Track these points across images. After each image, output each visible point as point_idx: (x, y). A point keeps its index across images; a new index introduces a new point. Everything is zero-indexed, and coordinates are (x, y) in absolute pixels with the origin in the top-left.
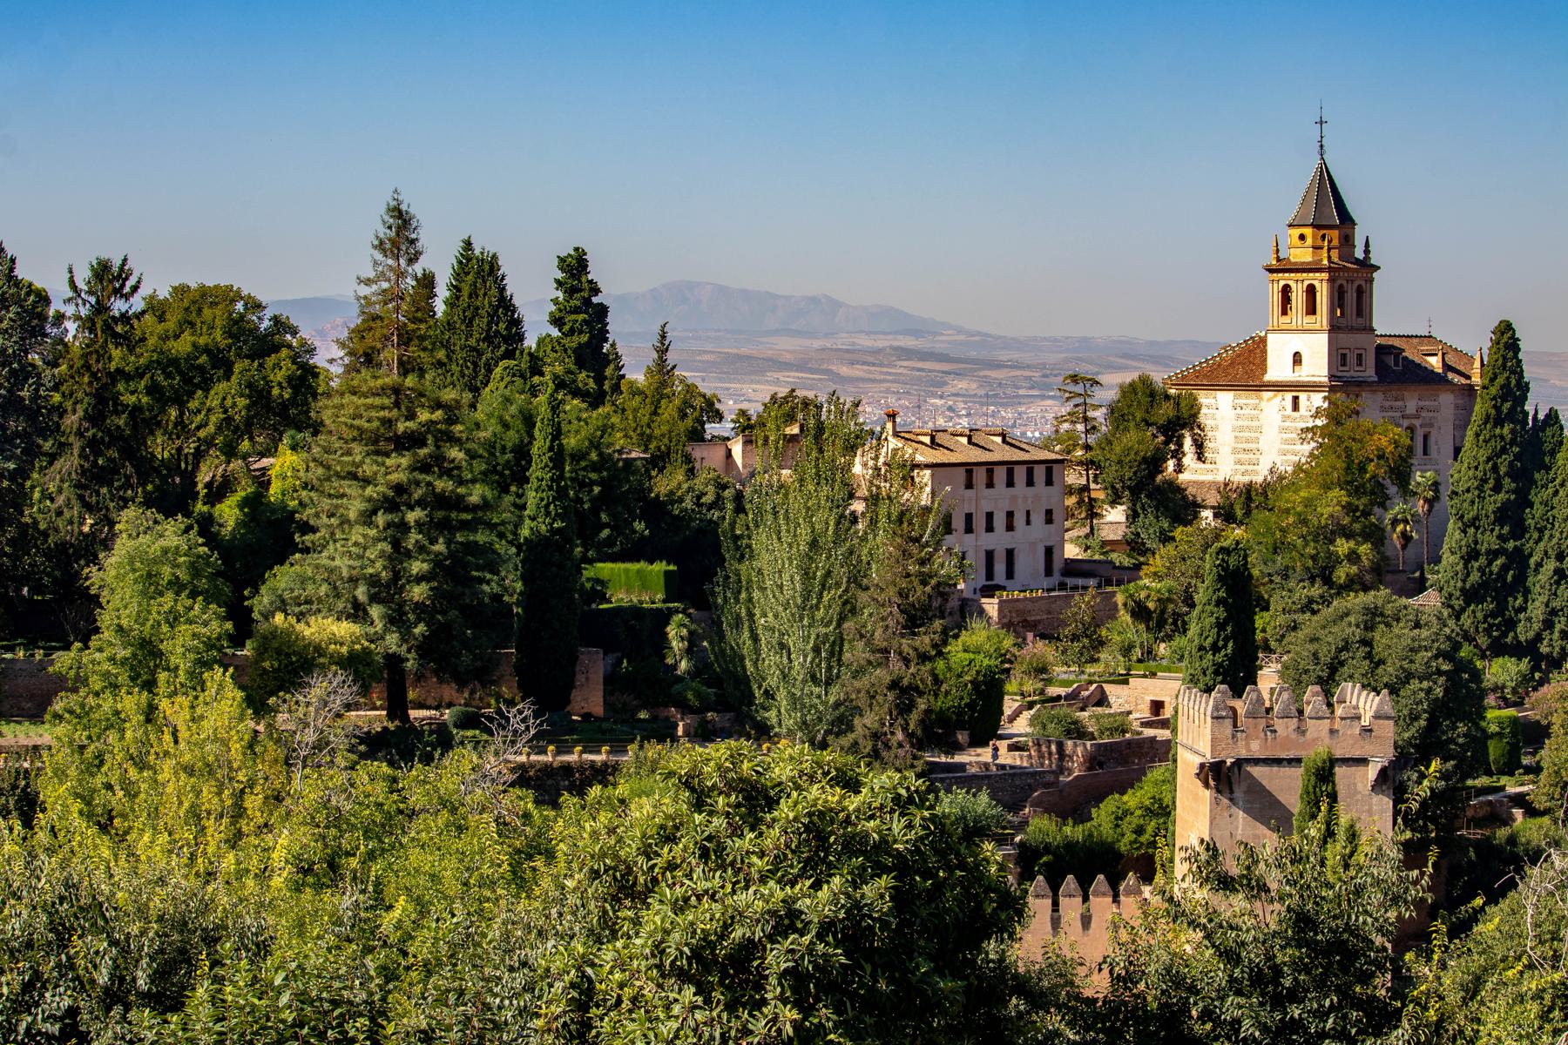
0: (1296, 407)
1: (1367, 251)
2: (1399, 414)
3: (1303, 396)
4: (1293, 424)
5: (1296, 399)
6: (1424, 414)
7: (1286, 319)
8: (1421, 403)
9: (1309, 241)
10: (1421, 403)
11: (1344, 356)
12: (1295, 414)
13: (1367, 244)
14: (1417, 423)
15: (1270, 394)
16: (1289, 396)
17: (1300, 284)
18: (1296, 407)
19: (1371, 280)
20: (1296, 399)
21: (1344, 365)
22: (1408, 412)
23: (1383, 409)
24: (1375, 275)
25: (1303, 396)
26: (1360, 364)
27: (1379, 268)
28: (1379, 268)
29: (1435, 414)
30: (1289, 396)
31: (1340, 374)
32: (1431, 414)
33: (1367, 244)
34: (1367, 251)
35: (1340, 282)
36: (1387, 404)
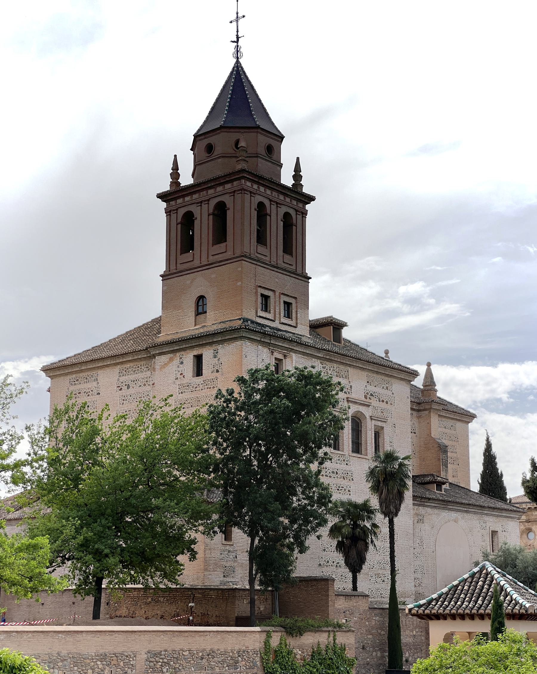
0: (199, 372)
1: (297, 176)
3: (207, 354)
4: (194, 395)
5: (199, 359)
6: (374, 402)
7: (188, 256)
8: (371, 389)
9: (218, 151)
10: (371, 389)
11: (266, 298)
12: (199, 380)
13: (297, 169)
14: (367, 412)
15: (164, 359)
16: (189, 358)
17: (205, 206)
18: (199, 372)
19: (304, 213)
20: (199, 359)
21: (266, 308)
24: (308, 207)
25: (207, 354)
26: (288, 315)
27: (311, 199)
28: (312, 199)
29: (388, 407)
30: (189, 358)
31: (259, 320)
32: (383, 405)
33: (297, 169)
34: (297, 176)
35: (259, 199)
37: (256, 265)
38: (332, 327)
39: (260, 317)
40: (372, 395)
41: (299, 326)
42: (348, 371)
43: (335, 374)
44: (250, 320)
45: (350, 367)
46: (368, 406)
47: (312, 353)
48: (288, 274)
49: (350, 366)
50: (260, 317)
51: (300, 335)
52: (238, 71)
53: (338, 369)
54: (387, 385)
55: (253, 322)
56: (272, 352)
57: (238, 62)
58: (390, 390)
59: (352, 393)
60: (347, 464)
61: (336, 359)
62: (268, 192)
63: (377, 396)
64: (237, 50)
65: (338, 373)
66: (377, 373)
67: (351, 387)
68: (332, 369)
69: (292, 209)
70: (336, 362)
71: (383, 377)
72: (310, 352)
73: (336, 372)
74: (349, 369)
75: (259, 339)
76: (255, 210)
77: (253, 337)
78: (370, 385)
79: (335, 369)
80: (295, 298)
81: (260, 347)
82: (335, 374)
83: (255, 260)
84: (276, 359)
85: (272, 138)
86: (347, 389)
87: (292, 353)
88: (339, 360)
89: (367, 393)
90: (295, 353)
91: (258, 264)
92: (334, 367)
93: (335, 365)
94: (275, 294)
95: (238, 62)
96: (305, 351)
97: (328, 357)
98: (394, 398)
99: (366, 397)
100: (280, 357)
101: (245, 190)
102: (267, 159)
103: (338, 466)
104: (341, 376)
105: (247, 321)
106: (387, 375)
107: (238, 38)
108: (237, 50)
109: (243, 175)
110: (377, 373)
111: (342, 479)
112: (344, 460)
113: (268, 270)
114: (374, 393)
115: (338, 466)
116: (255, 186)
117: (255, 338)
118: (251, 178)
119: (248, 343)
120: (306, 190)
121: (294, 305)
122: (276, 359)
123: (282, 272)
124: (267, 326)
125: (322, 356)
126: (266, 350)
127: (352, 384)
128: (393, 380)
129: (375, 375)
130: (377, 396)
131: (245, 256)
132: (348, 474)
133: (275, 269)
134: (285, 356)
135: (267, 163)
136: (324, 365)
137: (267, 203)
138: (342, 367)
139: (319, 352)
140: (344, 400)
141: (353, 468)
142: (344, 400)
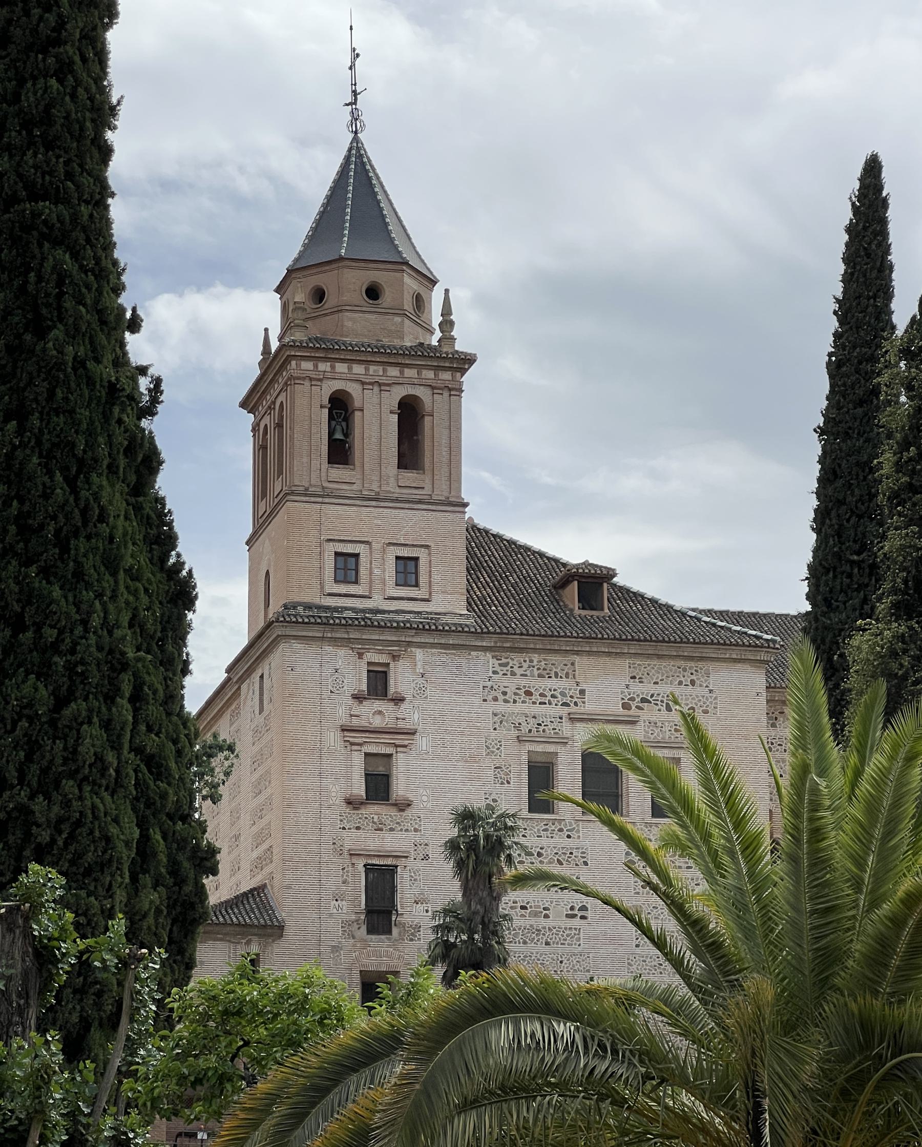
2: (555, 710)
6: (648, 714)
10: (638, 689)
19: (456, 390)
22: (589, 707)
23: (493, 694)
33: (447, 310)
34: (447, 324)
35: (337, 385)
36: (510, 683)
37: (322, 503)
38: (576, 583)
39: (330, 595)
40: (644, 700)
41: (435, 597)
42: (573, 664)
43: (536, 672)
44: (300, 604)
45: (577, 654)
46: (633, 723)
47: (461, 642)
48: (407, 506)
49: (577, 653)
50: (330, 595)
51: (436, 614)
52: (360, 156)
53: (543, 663)
54: (693, 677)
55: (320, 607)
56: (360, 655)
57: (356, 139)
58: (701, 686)
59: (584, 703)
60: (569, 837)
61: (532, 646)
62: (358, 369)
63: (662, 701)
64: (355, 118)
65: (544, 669)
66: (658, 658)
67: (582, 692)
68: (525, 665)
69: (422, 388)
70: (535, 650)
71: (682, 663)
72: (456, 642)
73: (538, 669)
74: (577, 659)
75: (320, 635)
76: (322, 407)
77: (300, 634)
78: (640, 682)
79: (535, 663)
80: (427, 547)
81: (328, 649)
82: (536, 672)
83: (319, 496)
84: (369, 664)
85: (381, 270)
86: (571, 697)
87: (413, 649)
88: (541, 647)
89: (632, 699)
90: (419, 647)
91: (327, 500)
92: (531, 661)
93: (536, 658)
94: (371, 548)
95: (356, 139)
96: (443, 641)
97: (508, 645)
98: (716, 698)
99: (626, 706)
100: (383, 659)
101: (295, 378)
102: (364, 309)
103: (544, 842)
104: (553, 676)
105: (295, 608)
106: (691, 658)
107: (355, 93)
108: (355, 118)
109: (288, 353)
110: (660, 657)
111: (556, 864)
112: (561, 830)
113: (355, 508)
114: (652, 696)
115: (544, 842)
116: (322, 366)
117: (310, 634)
118: (308, 354)
119: (297, 645)
120: (458, 347)
121: (422, 563)
122: (369, 664)
123: (391, 505)
124: (346, 609)
125: (492, 644)
126: (342, 652)
127: (583, 686)
128: (711, 666)
129: (655, 662)
130: (662, 701)
131: (292, 493)
132: (571, 853)
133: (374, 503)
134: (395, 658)
135: (367, 316)
136: (504, 661)
137: (354, 389)
138: (553, 658)
139: (483, 639)
140: (561, 718)
141: (587, 843)
142: (561, 718)
